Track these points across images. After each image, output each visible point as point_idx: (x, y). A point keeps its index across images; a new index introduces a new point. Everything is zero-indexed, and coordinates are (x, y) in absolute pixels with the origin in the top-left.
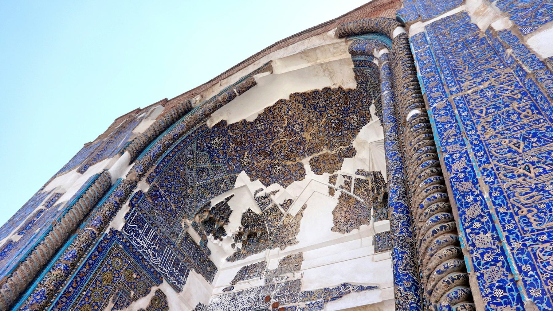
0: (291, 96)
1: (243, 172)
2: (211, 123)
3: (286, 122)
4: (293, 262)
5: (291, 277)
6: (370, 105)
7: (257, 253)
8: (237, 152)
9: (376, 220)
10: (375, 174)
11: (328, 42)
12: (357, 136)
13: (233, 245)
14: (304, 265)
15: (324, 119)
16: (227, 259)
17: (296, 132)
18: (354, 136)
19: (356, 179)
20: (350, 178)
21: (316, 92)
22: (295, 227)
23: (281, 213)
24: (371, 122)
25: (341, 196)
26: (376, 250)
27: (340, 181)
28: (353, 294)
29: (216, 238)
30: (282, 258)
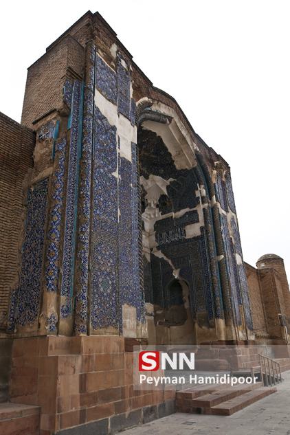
0: (159, 137)
15: (154, 156)
18: (154, 174)
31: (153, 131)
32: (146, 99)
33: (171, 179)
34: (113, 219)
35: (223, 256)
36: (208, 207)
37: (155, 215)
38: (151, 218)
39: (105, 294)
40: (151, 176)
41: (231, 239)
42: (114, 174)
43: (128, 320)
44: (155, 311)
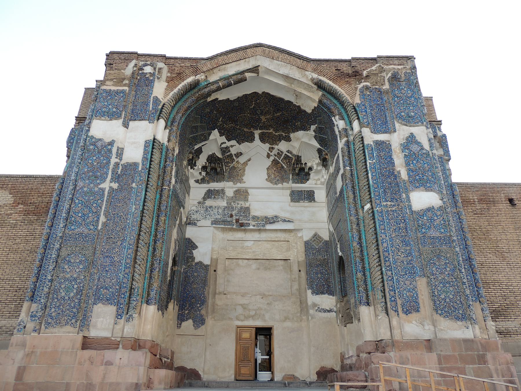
0: (263, 93)
1: (216, 130)
2: (209, 99)
3: (253, 105)
4: (242, 194)
5: (243, 204)
6: (313, 125)
7: (217, 182)
8: (216, 116)
9: (293, 183)
10: (298, 156)
11: (304, 80)
12: (296, 133)
13: (200, 173)
14: (250, 198)
16: (195, 181)
17: (257, 113)
18: (294, 132)
19: (285, 154)
20: (282, 152)
21: (282, 100)
22: (242, 171)
23: (234, 159)
24: (308, 132)
25: (273, 160)
26: (292, 200)
27: (275, 152)
28: (280, 222)
29: (191, 168)
30: (234, 189)
31: (249, 93)
32: (190, 79)
33: (313, 127)
34: (92, 227)
35: (368, 206)
36: (348, 143)
37: (323, 176)
38: (322, 183)
39: (67, 298)
40: (292, 135)
41: (399, 172)
42: (102, 186)
43: (102, 319)
44: (336, 306)
